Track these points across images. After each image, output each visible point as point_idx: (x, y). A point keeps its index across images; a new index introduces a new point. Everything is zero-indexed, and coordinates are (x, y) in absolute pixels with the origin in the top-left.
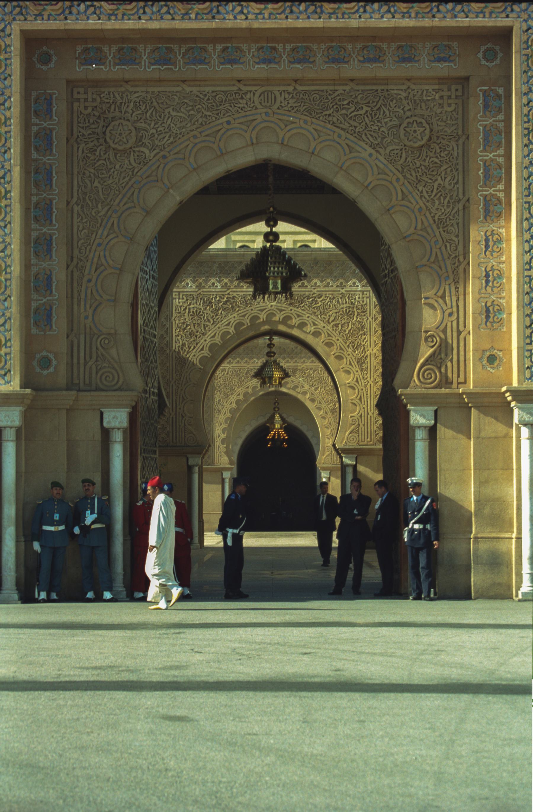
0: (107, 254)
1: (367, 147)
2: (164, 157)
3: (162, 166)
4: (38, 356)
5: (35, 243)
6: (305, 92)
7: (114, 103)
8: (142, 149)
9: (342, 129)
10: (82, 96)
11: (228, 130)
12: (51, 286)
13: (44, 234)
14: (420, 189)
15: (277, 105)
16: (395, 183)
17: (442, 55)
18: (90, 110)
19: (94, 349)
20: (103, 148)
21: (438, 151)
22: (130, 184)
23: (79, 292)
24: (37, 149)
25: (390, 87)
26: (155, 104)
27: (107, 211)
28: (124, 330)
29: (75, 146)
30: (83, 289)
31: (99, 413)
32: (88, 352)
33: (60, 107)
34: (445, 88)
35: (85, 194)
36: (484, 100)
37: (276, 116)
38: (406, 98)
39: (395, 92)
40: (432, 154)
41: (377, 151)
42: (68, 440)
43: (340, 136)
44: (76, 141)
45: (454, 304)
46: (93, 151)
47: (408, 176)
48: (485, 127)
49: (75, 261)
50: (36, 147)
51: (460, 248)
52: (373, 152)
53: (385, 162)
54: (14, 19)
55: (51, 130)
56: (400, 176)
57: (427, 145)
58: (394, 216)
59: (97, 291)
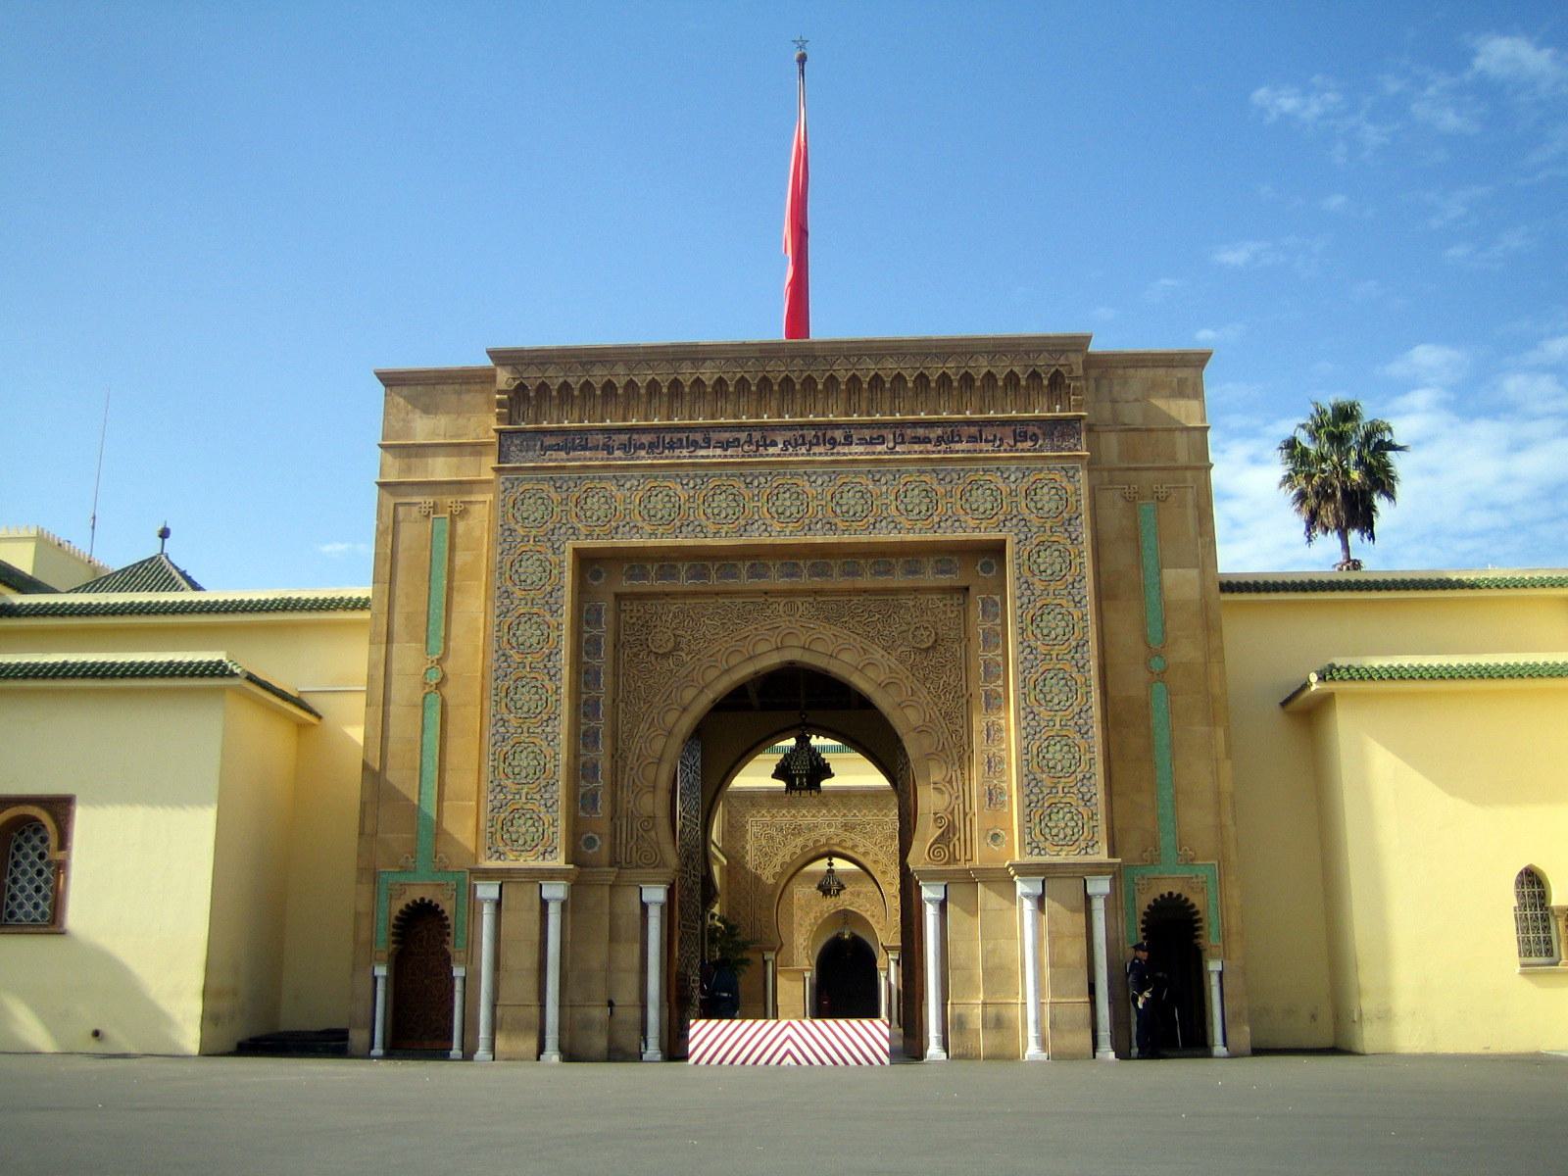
1: (879, 650)
2: (699, 659)
4: (584, 837)
5: (584, 735)
9: (858, 634)
15: (800, 613)
17: (945, 568)
18: (634, 620)
20: (645, 652)
21: (943, 652)
23: (623, 779)
24: (587, 653)
25: (900, 597)
26: (691, 613)
28: (662, 814)
29: (622, 651)
31: (639, 889)
33: (607, 617)
35: (629, 692)
36: (983, 606)
38: (914, 606)
42: (611, 913)
43: (855, 639)
44: (623, 646)
46: (636, 655)
47: (917, 674)
48: (984, 630)
49: (619, 751)
51: (965, 737)
52: (885, 653)
54: (568, 539)
55: (600, 637)
57: (933, 647)
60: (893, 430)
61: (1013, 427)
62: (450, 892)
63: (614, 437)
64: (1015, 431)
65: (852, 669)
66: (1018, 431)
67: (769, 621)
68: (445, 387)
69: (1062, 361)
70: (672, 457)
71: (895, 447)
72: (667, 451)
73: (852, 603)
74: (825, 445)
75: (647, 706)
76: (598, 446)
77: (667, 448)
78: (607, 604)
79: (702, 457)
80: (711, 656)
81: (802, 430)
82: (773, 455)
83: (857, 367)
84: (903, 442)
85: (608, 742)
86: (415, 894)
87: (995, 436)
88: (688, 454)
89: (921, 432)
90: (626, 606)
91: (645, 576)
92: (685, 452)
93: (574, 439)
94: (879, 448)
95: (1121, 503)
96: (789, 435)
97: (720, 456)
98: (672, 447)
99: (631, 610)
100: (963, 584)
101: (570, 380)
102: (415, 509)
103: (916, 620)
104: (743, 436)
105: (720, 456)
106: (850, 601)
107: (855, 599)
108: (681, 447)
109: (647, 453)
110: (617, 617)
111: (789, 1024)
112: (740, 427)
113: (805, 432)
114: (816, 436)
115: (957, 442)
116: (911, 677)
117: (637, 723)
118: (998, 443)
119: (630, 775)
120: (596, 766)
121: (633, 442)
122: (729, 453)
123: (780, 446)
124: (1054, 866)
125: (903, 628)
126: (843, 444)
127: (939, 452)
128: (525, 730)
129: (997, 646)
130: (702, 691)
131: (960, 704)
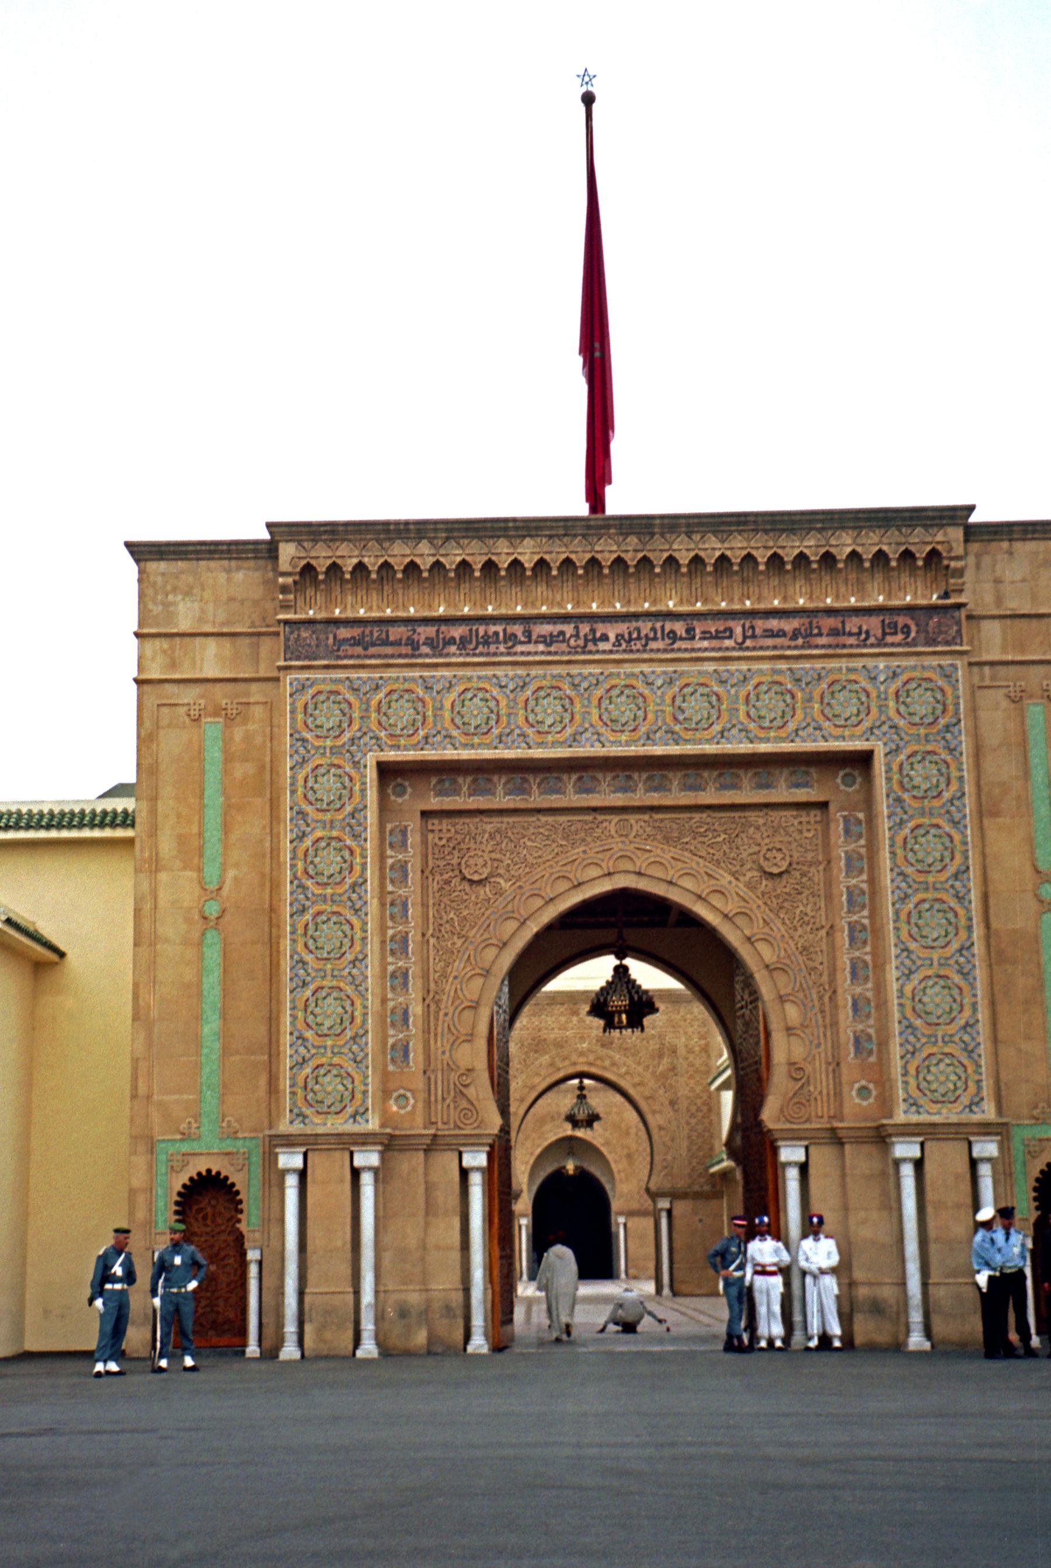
1: (726, 875)
2: (520, 887)
3: (518, 897)
4: (395, 1094)
6: (662, 820)
7: (469, 833)
9: (700, 857)
10: (436, 828)
11: (584, 859)
13: (400, 968)
15: (633, 834)
16: (756, 911)
18: (444, 842)
20: (458, 879)
24: (392, 881)
26: (510, 834)
30: (440, 1023)
31: (456, 1154)
32: (445, 1089)
33: (413, 839)
34: (804, 813)
35: (441, 925)
37: (633, 845)
38: (764, 824)
40: (791, 881)
41: (737, 879)
42: (426, 1182)
43: (698, 863)
44: (431, 872)
45: (821, 1035)
46: (448, 882)
47: (769, 903)
48: (846, 852)
52: (732, 879)
53: (745, 889)
54: (370, 750)
55: (406, 862)
56: (760, 903)
60: (742, 622)
61: (881, 618)
62: (241, 1161)
63: (420, 629)
64: (883, 621)
66: (887, 621)
67: (599, 843)
68: (212, 564)
69: (939, 537)
70: (488, 654)
71: (744, 642)
72: (481, 646)
74: (663, 639)
76: (401, 639)
78: (413, 824)
79: (522, 653)
80: (533, 883)
82: (604, 652)
83: (701, 546)
84: (754, 636)
85: (419, 982)
86: (201, 1166)
87: (860, 628)
89: (774, 624)
90: (434, 823)
91: (457, 792)
93: (371, 632)
94: (728, 643)
95: (1005, 703)
96: (623, 628)
97: (542, 653)
99: (440, 831)
100: (822, 798)
101: (366, 560)
102: (182, 710)
103: (767, 841)
104: (569, 629)
105: (542, 653)
106: (691, 819)
107: (697, 816)
108: (498, 642)
109: (458, 649)
110: (424, 842)
112: (566, 618)
113: (640, 624)
114: (653, 629)
116: (763, 907)
117: (451, 961)
118: (863, 636)
119: (444, 1022)
120: (406, 1013)
121: (441, 636)
122: (552, 649)
124: (934, 1125)
126: (685, 639)
127: (796, 647)
128: (329, 972)
129: (861, 871)
130: (523, 923)
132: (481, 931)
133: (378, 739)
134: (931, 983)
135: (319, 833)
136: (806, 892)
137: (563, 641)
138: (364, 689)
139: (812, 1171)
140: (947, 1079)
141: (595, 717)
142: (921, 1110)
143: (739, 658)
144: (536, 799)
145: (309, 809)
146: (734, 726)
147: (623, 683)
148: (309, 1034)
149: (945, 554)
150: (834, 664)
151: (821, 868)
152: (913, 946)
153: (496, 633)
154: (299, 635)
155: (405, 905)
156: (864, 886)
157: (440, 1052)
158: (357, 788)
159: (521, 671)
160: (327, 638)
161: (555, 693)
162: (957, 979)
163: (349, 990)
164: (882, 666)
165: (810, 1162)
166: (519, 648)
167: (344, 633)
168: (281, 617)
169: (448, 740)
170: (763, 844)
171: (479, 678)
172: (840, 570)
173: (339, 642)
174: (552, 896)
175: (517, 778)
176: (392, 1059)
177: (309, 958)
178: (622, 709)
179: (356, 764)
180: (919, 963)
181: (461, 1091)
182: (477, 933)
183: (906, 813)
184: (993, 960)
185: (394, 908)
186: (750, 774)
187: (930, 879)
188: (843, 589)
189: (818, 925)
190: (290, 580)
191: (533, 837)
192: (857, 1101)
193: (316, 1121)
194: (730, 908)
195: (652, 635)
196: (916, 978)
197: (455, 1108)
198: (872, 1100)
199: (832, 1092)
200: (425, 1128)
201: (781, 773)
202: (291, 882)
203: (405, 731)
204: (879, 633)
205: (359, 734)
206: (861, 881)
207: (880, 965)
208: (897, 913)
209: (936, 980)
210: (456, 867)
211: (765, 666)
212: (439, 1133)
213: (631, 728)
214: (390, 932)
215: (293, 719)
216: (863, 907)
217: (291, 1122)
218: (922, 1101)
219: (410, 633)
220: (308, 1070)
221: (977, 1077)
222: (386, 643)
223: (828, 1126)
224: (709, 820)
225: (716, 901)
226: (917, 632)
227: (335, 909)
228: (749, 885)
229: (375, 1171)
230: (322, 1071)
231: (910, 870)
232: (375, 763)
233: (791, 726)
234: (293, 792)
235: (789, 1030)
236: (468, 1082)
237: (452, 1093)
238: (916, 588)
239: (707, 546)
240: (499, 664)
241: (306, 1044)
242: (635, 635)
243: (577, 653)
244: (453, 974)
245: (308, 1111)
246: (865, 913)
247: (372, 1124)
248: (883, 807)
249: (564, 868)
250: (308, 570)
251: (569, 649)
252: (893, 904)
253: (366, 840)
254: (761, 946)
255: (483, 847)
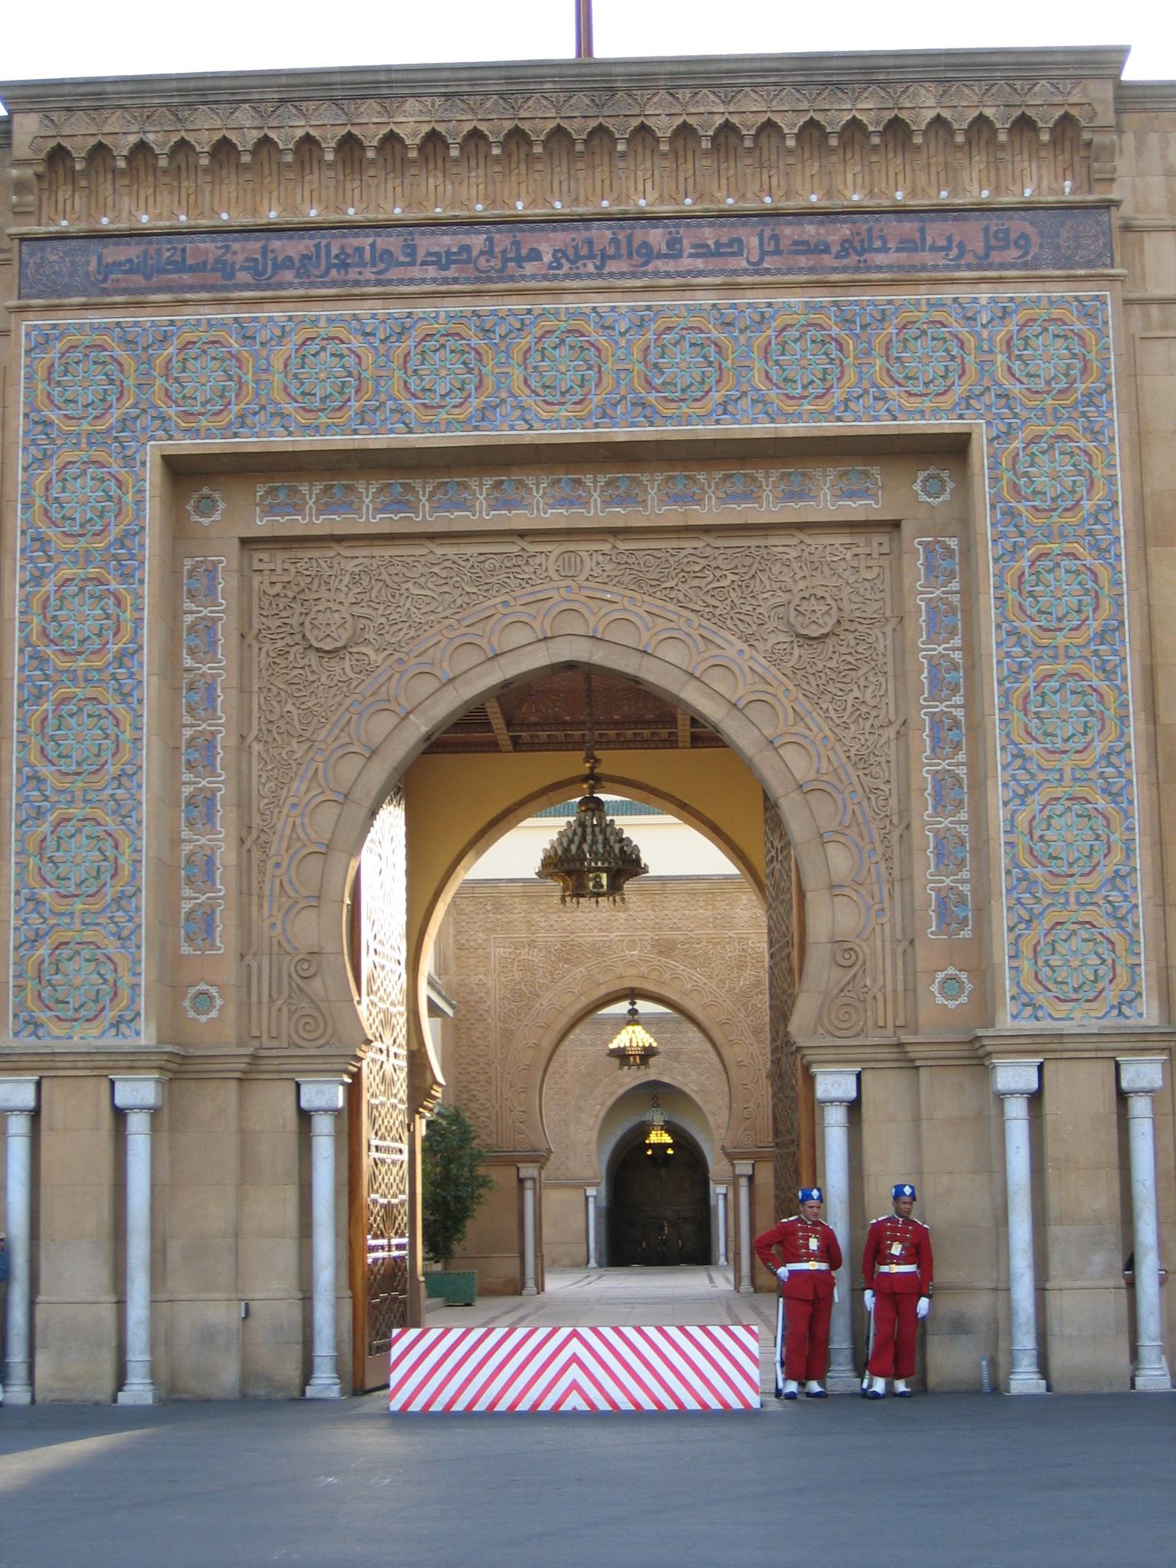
0: (307, 821)
3: (397, 675)
4: (192, 991)
5: (188, 804)
8: (364, 650)
12: (214, 873)
14: (825, 706)
17: (854, 487)
18: (278, 588)
19: (285, 979)
21: (853, 643)
22: (345, 706)
23: (261, 883)
24: (192, 652)
27: (307, 751)
29: (256, 646)
30: (268, 879)
31: (293, 1086)
33: (226, 583)
34: (861, 540)
36: (926, 558)
37: (585, 592)
39: (781, 549)
42: (242, 1131)
45: (886, 895)
48: (928, 601)
49: (255, 833)
50: (190, 648)
51: (893, 802)
52: (745, 647)
53: (764, 662)
54: (152, 438)
58: (781, 751)
59: (291, 882)
63: (235, 246)
64: (986, 230)
65: (685, 677)
67: (531, 590)
69: (1075, 98)
70: (345, 283)
71: (761, 260)
72: (334, 272)
73: (684, 553)
74: (630, 256)
75: (306, 746)
76: (205, 263)
77: (335, 266)
78: (227, 558)
81: (587, 229)
82: (533, 277)
84: (777, 252)
85: (233, 815)
87: (950, 239)
88: (373, 277)
89: (810, 230)
90: (262, 558)
91: (298, 508)
92: (368, 274)
93: (159, 252)
96: (561, 238)
97: (434, 280)
98: (344, 265)
101: (151, 137)
103: (802, 585)
105: (434, 280)
107: (688, 545)
108: (362, 264)
109: (297, 276)
111: (575, 1334)
112: (472, 224)
114: (614, 241)
115: (877, 250)
118: (955, 252)
120: (210, 861)
123: (547, 258)
125: (776, 600)
126: (666, 256)
127: (845, 269)
128: (79, 794)
129: (953, 633)
130: (405, 718)
131: (883, 740)
132: (336, 731)
133: (164, 419)
134: (1059, 808)
135: (67, 572)
136: (865, 668)
137: (468, 261)
138: (142, 342)
139: (867, 1111)
140: (1084, 963)
141: (517, 383)
142: (1040, 1014)
143: (753, 286)
144: (427, 517)
145: (51, 533)
146: (744, 394)
147: (563, 326)
148: (46, 893)
149: (1083, 123)
150: (902, 295)
151: (889, 629)
152: (1031, 748)
153: (359, 250)
154: (42, 258)
155: (211, 688)
156: (957, 656)
157: (267, 923)
158: (129, 498)
159: (398, 310)
160: (88, 263)
161: (452, 343)
162: (1101, 802)
163: (111, 823)
164: (984, 298)
165: (865, 1099)
166: (394, 273)
167: (114, 253)
168: (13, 230)
169: (278, 420)
170: (795, 591)
171: (330, 320)
172: (918, 148)
173: (105, 269)
174: (451, 676)
175: (397, 483)
176: (187, 935)
177: (46, 771)
178: (564, 367)
179: (128, 461)
180: (1041, 776)
181: (298, 986)
182: (326, 737)
183: (1022, 534)
184: (1161, 776)
185: (185, 691)
186: (775, 474)
187: (1061, 639)
188: (922, 178)
189: (882, 720)
190: (29, 172)
191: (422, 580)
192: (940, 1000)
193: (57, 1032)
194: (739, 693)
195: (611, 251)
196: (1037, 799)
197: (290, 1012)
198: (963, 999)
199: (900, 987)
200: (240, 1045)
201: (825, 476)
202: (21, 651)
203: (208, 407)
204: (979, 247)
205: (135, 412)
206: (952, 648)
207: (978, 784)
208: (1006, 695)
209: (1068, 804)
210: (297, 629)
211: (795, 299)
212: (262, 1053)
213: (576, 398)
214: (187, 733)
215: (30, 389)
216: (955, 690)
217: (16, 1034)
218: (1041, 999)
219: (221, 251)
220: (43, 951)
221: (1132, 960)
222: (180, 267)
223: (894, 1041)
224: (708, 551)
225: (719, 682)
226: (1041, 246)
227: (91, 692)
228: (773, 659)
229: (154, 1113)
230: (66, 952)
231: (1027, 627)
232: (159, 458)
233: (838, 394)
234: (27, 506)
235: (833, 888)
236: (312, 971)
237: (286, 994)
238: (1040, 178)
239: (701, 110)
240: (363, 297)
241: (41, 909)
242: (584, 252)
243: (490, 280)
244: (289, 801)
245: (43, 1016)
246: (958, 699)
247: (145, 1036)
248: (986, 525)
249: (470, 630)
250: (58, 155)
251: (477, 274)
252: (1000, 683)
253: (141, 582)
254: (791, 754)
255: (341, 597)
